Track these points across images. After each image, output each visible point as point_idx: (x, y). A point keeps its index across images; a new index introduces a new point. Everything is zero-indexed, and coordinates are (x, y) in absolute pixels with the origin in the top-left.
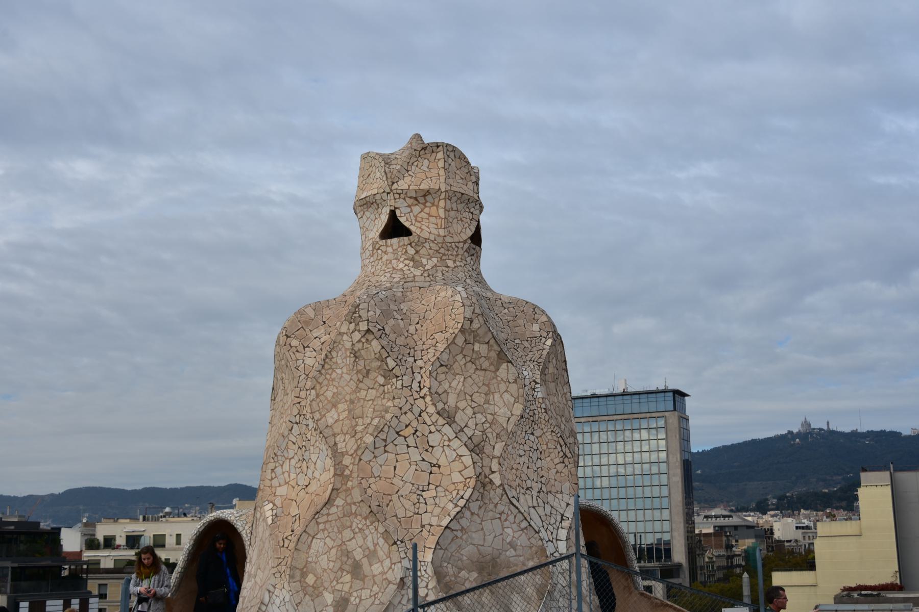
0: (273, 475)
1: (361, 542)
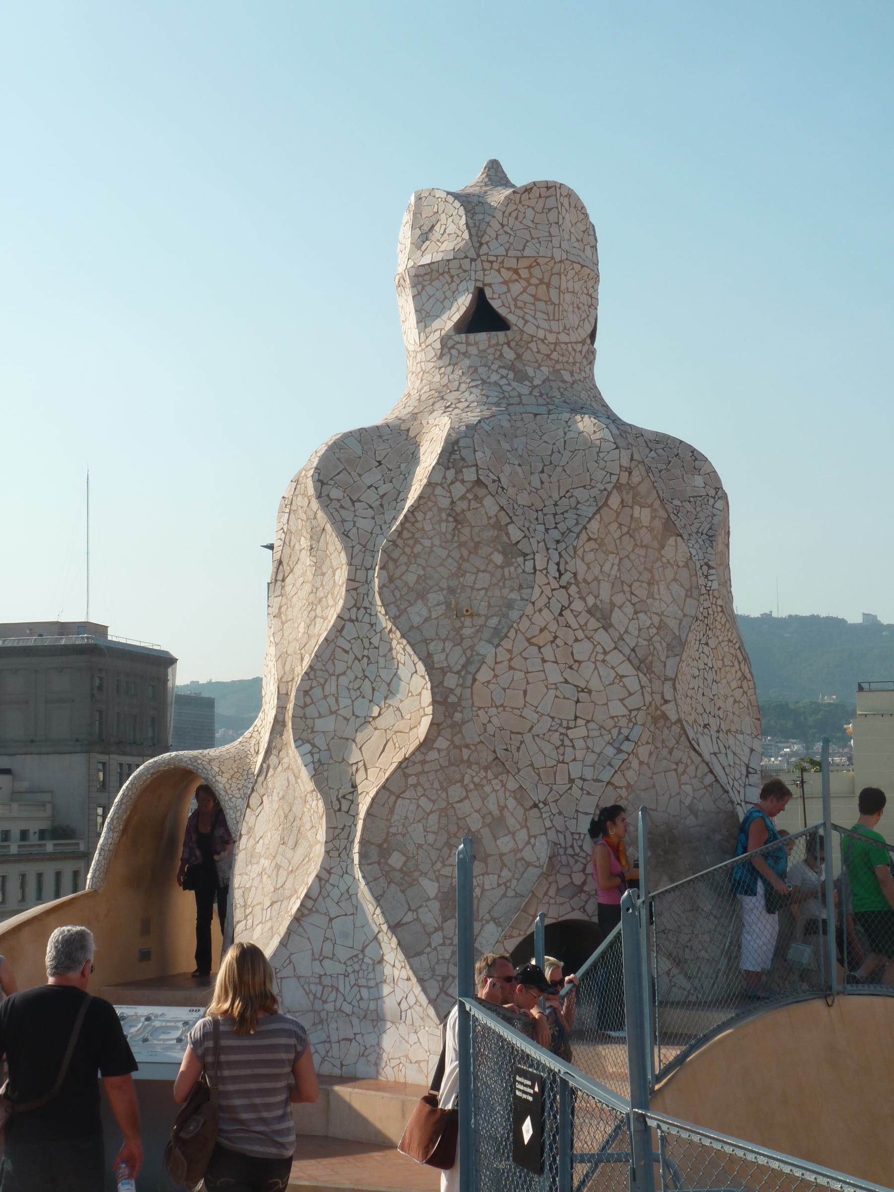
0: (308, 700)
1: (478, 804)
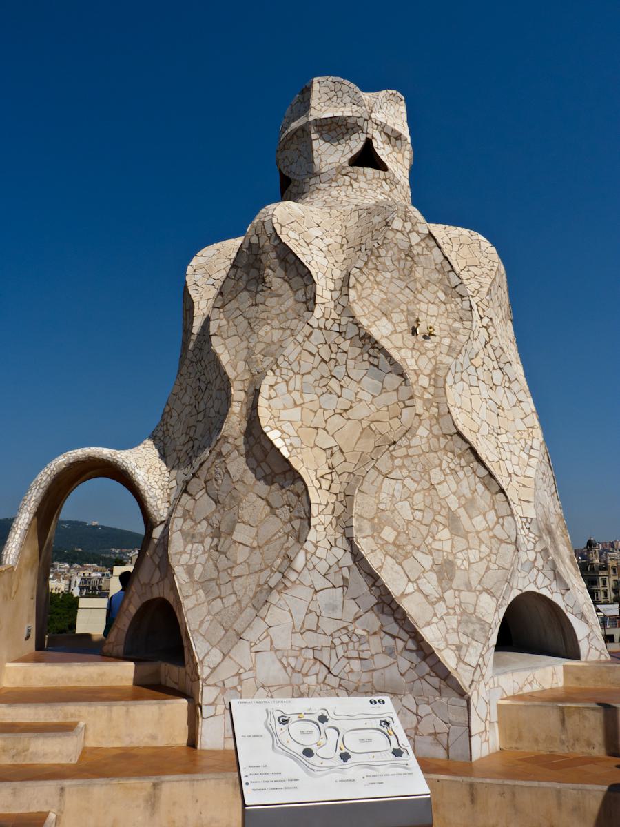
0: (273, 394)
1: (454, 487)
